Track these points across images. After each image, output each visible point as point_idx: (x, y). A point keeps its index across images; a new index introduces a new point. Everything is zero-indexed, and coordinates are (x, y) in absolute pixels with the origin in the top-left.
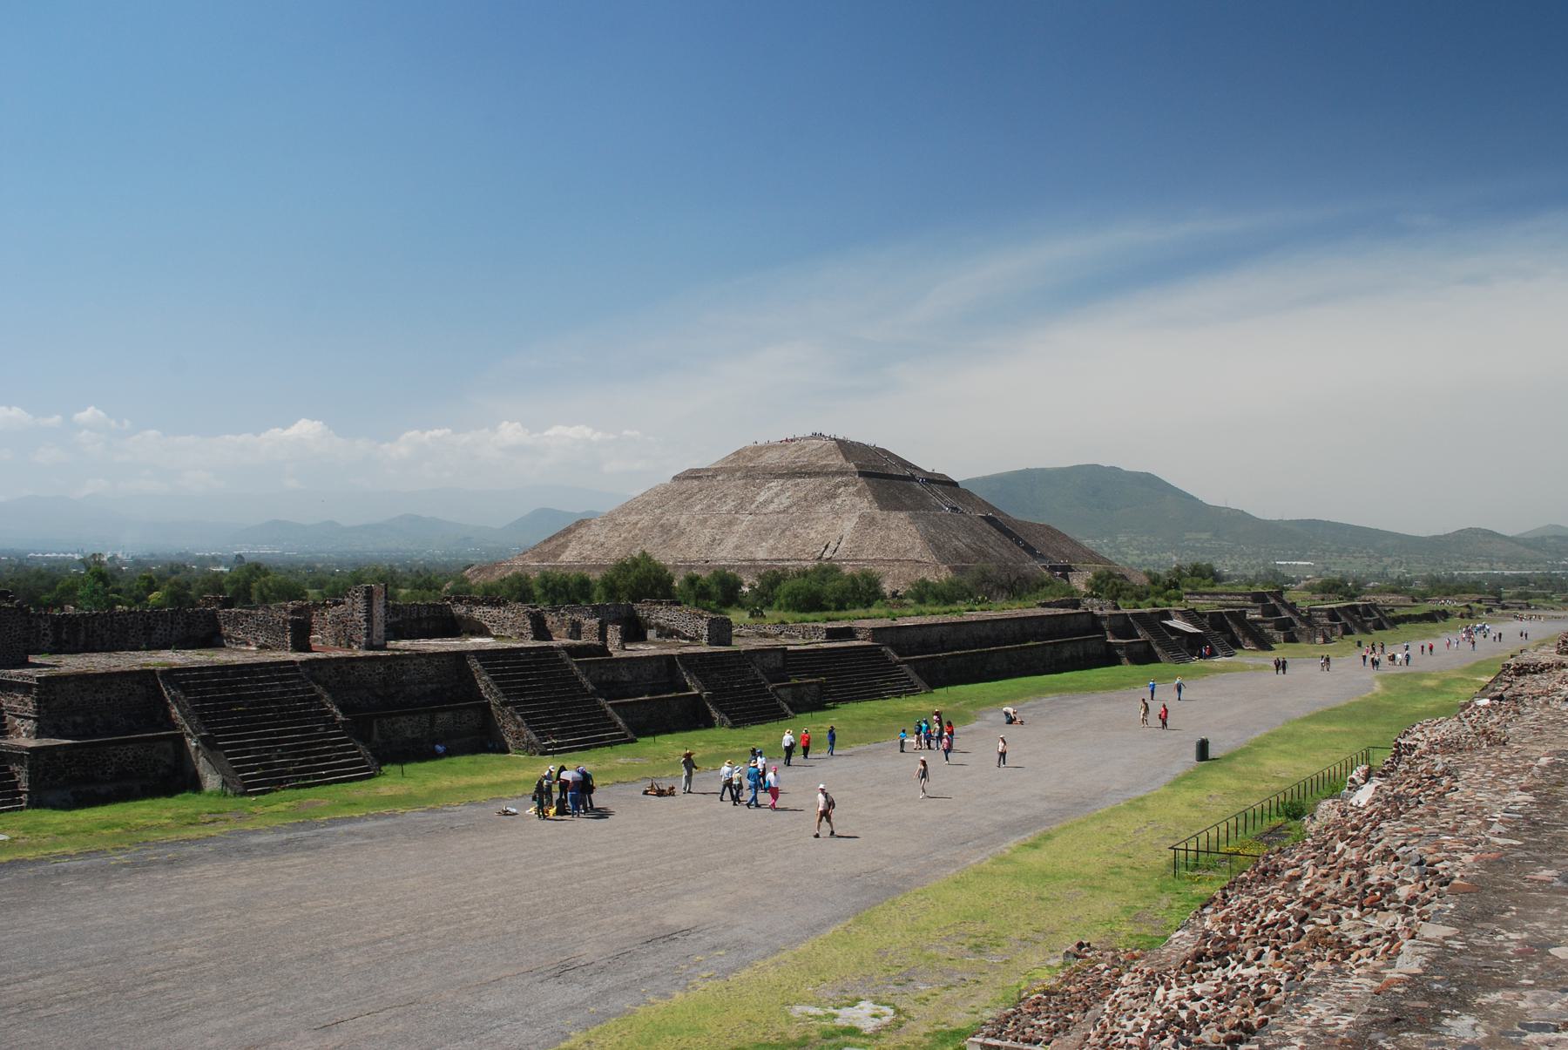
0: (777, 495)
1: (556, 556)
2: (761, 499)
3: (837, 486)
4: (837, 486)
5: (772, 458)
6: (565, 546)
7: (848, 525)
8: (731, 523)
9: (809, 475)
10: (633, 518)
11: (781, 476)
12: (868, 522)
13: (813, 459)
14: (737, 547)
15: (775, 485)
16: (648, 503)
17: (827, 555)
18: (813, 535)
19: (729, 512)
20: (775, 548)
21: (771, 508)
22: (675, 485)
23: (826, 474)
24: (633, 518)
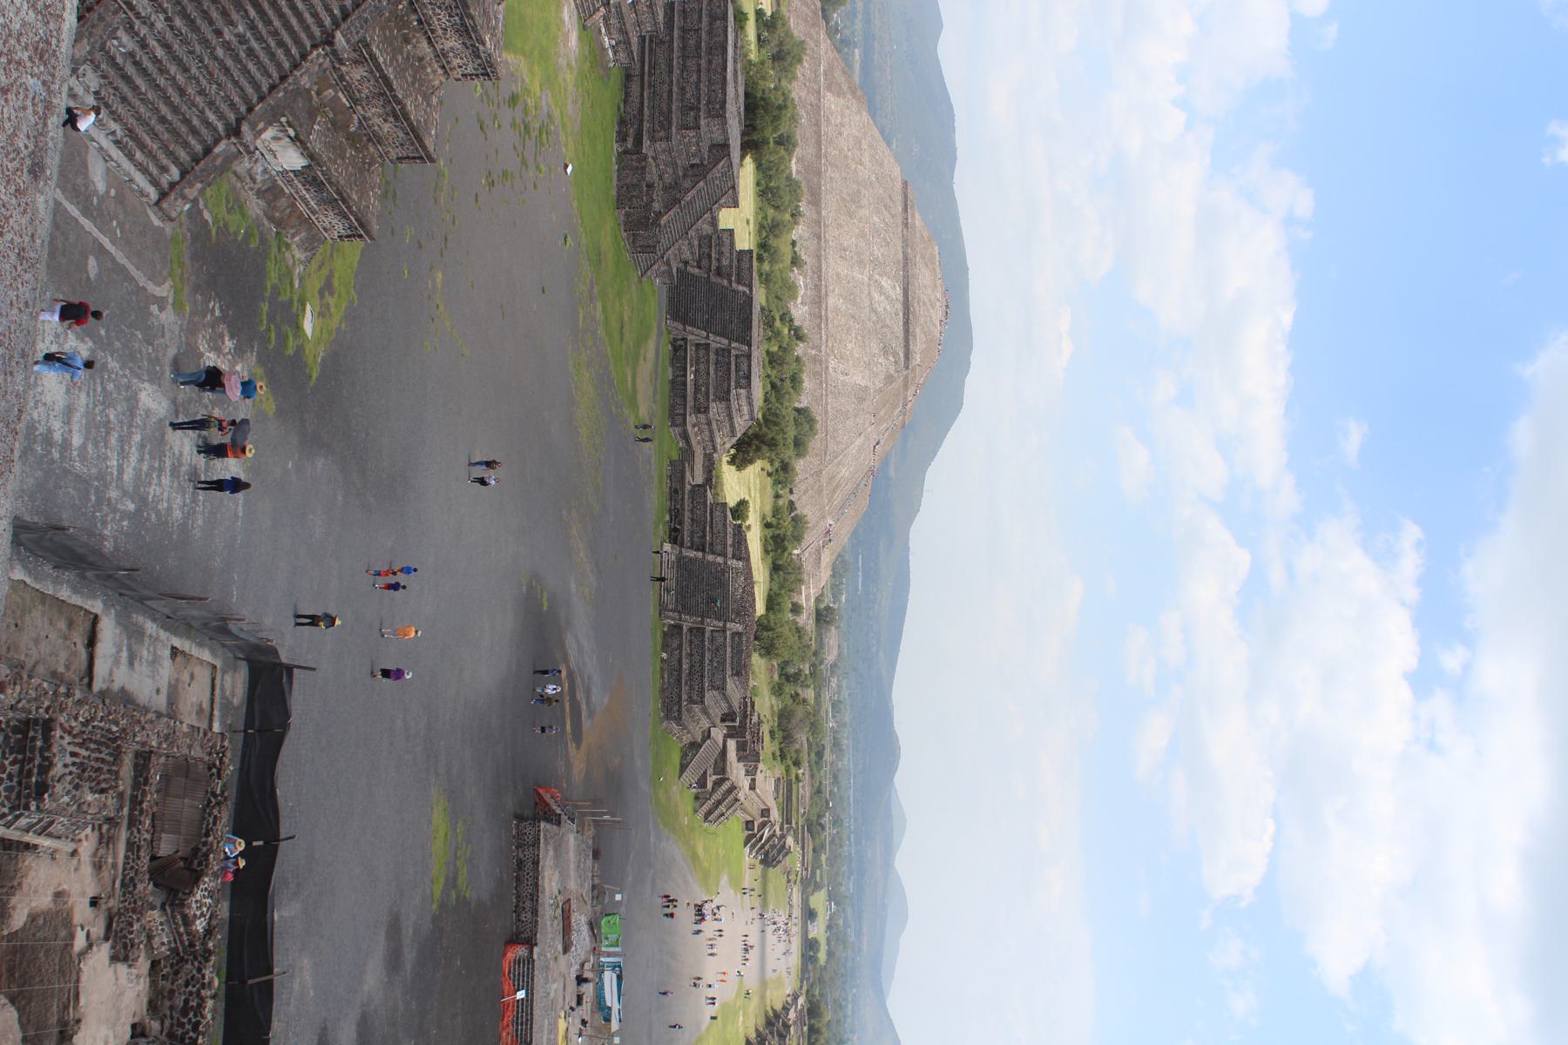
0: (887, 298)
1: (829, 88)
2: (886, 283)
3: (895, 354)
4: (895, 354)
5: (924, 277)
6: (840, 94)
7: (858, 378)
8: (861, 263)
9: (906, 323)
10: (866, 159)
11: (906, 291)
12: (861, 395)
13: (922, 320)
14: (838, 275)
15: (899, 290)
16: (881, 165)
17: (832, 363)
18: (850, 346)
19: (872, 254)
20: (837, 310)
21: (876, 296)
22: (899, 185)
23: (907, 340)
24: (866, 159)
